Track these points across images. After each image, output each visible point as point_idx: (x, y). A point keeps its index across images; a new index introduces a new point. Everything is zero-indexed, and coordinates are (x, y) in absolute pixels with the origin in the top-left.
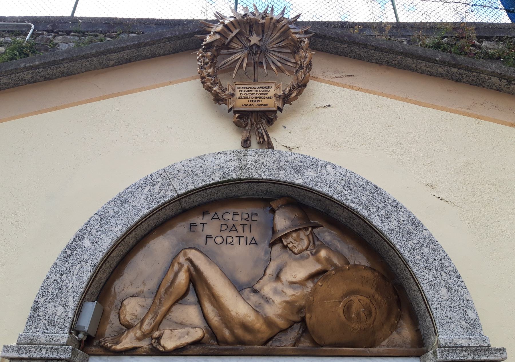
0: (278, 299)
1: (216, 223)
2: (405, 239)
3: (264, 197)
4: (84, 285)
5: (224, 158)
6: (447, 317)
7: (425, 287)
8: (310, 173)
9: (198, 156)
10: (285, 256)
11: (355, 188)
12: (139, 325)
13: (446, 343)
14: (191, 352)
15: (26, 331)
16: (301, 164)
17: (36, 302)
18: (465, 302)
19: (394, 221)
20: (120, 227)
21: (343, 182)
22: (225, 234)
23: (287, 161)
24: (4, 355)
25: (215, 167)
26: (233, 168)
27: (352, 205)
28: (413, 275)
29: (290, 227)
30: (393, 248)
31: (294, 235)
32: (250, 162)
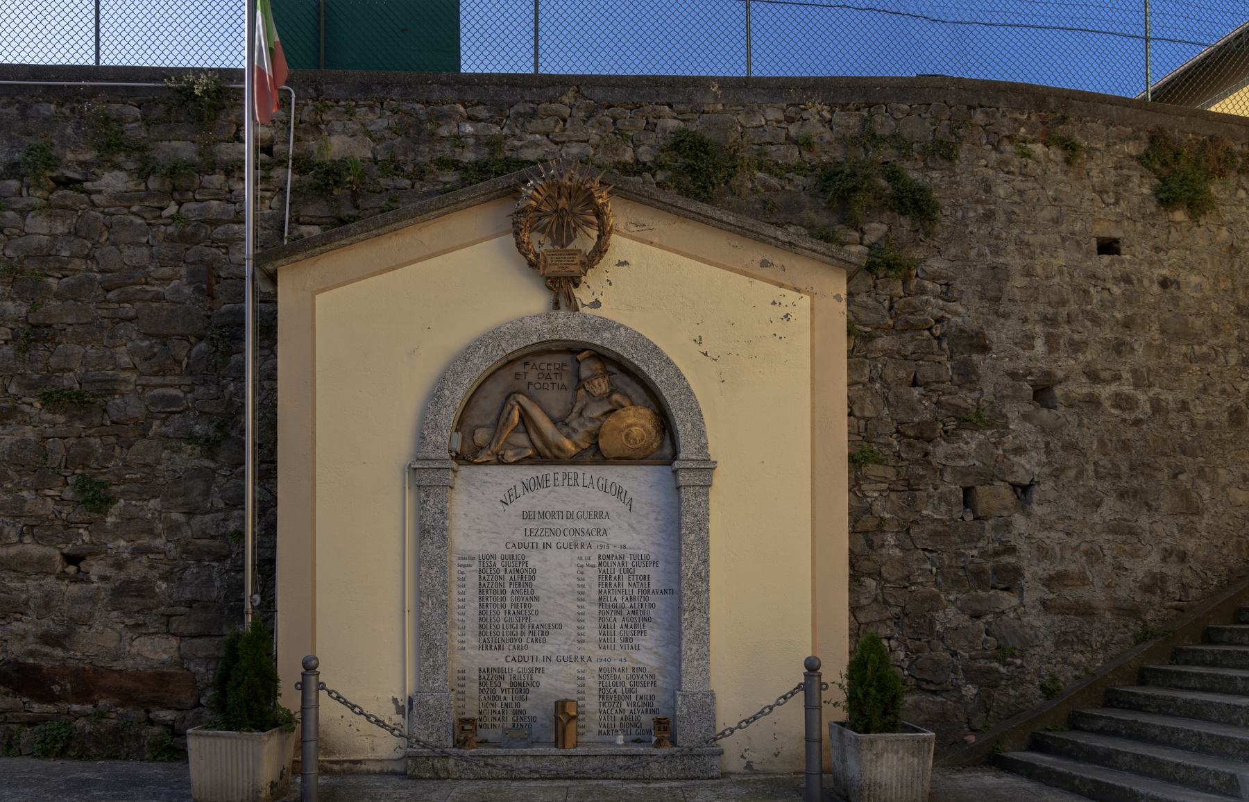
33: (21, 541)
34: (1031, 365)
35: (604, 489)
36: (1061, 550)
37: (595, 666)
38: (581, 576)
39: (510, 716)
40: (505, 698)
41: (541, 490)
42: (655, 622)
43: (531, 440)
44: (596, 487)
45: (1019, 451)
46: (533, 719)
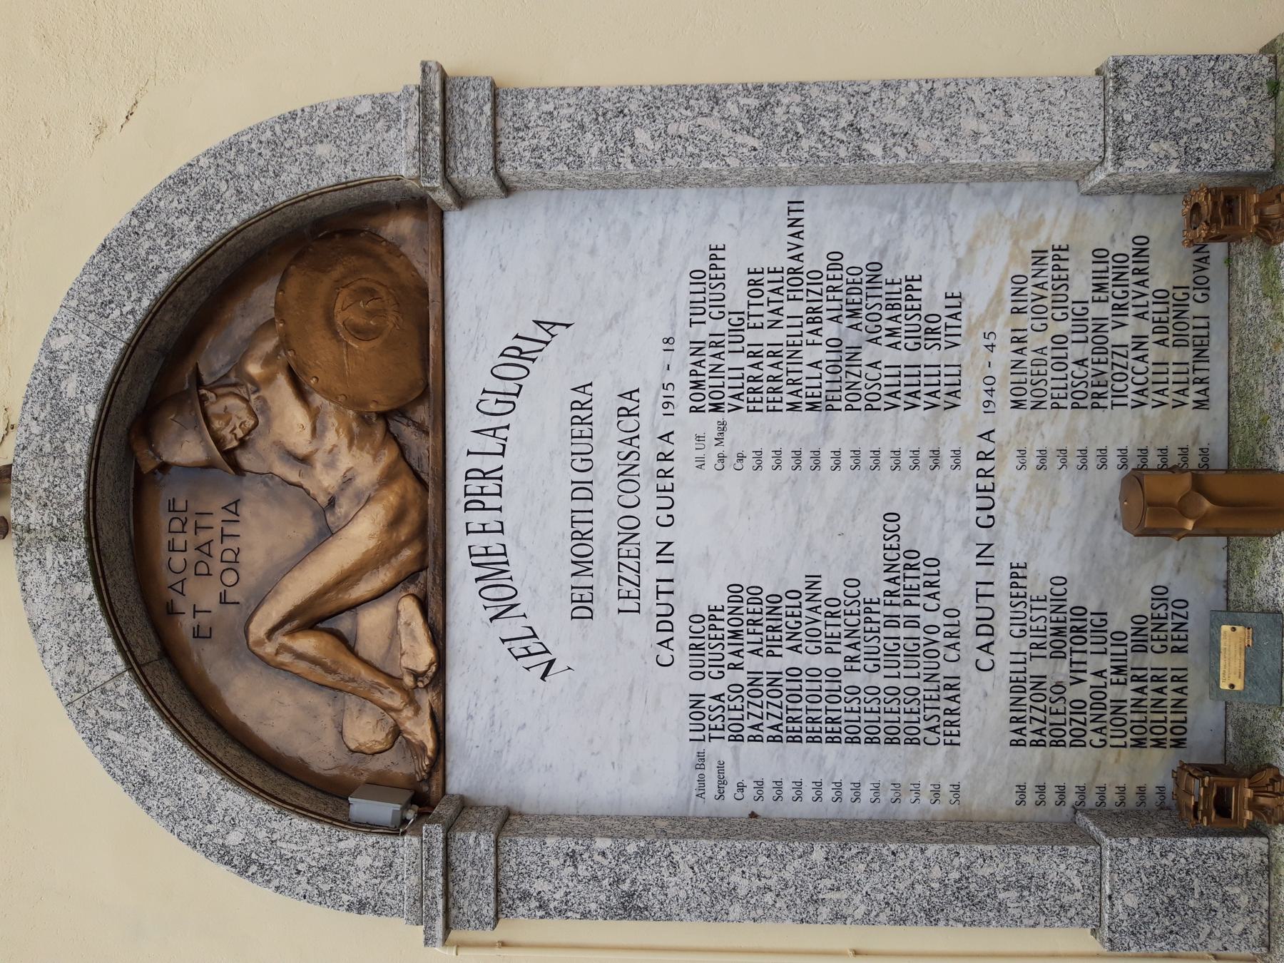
0: (346, 461)
1: (193, 586)
2: (219, 206)
3: (132, 486)
4: (318, 826)
5: (36, 576)
6: (368, 153)
7: (314, 184)
8: (70, 387)
9: (31, 636)
10: (262, 444)
11: (105, 292)
12: (393, 714)
13: (414, 166)
14: (439, 616)
15: (400, 913)
16: (48, 406)
17: (349, 909)
18: (342, 113)
19: (180, 220)
20: (200, 779)
21: (92, 317)
22: (217, 567)
23: (42, 436)
24: (439, 942)
25: (59, 595)
26: (60, 556)
27: (146, 303)
28: (293, 202)
29: (200, 433)
30: (237, 232)
31: (217, 424)
32: (46, 519)
35: (510, 399)
37: (1007, 420)
38: (750, 462)
39: (1151, 660)
40: (1099, 674)
41: (513, 570)
42: (883, 252)
44: (504, 421)
46: (1160, 594)
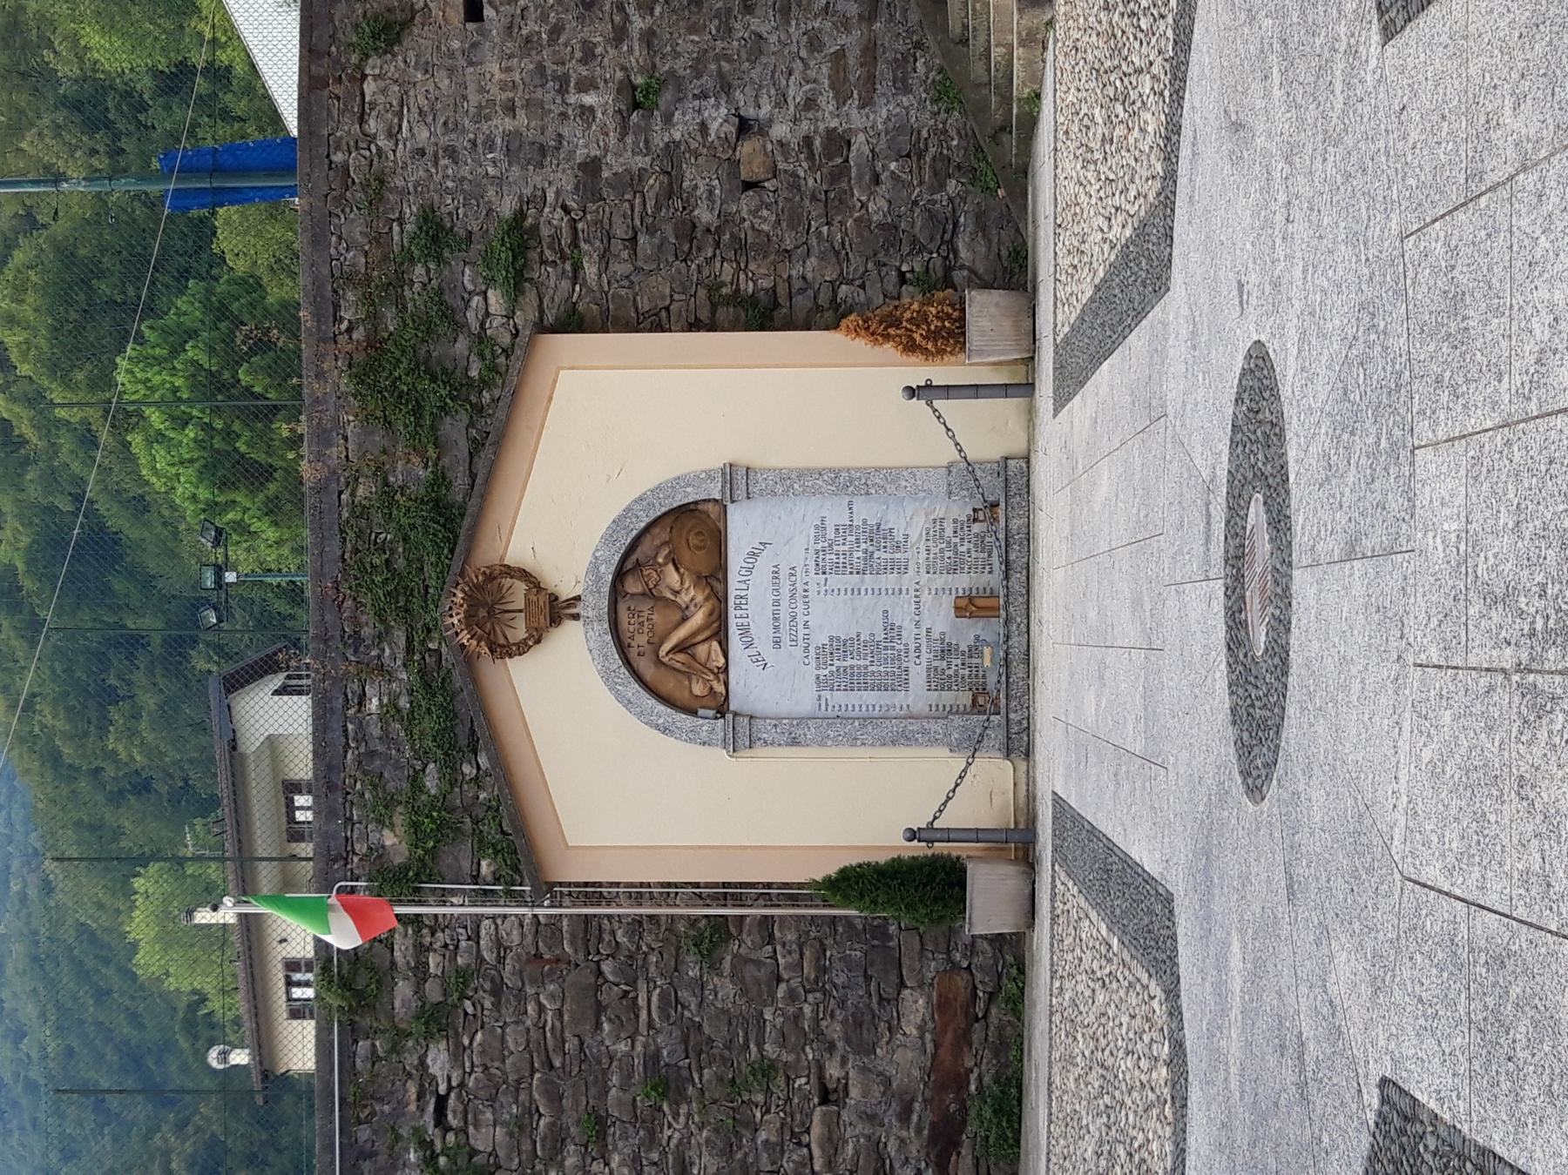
0: (692, 592)
5: (591, 633)
8: (603, 569)
33: (808, 1146)
34: (611, 112)
35: (750, 570)
36: (808, 82)
38: (836, 592)
43: (704, 641)
45: (704, 128)
46: (977, 638)
